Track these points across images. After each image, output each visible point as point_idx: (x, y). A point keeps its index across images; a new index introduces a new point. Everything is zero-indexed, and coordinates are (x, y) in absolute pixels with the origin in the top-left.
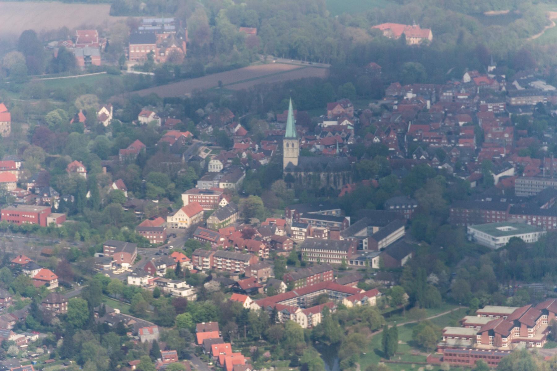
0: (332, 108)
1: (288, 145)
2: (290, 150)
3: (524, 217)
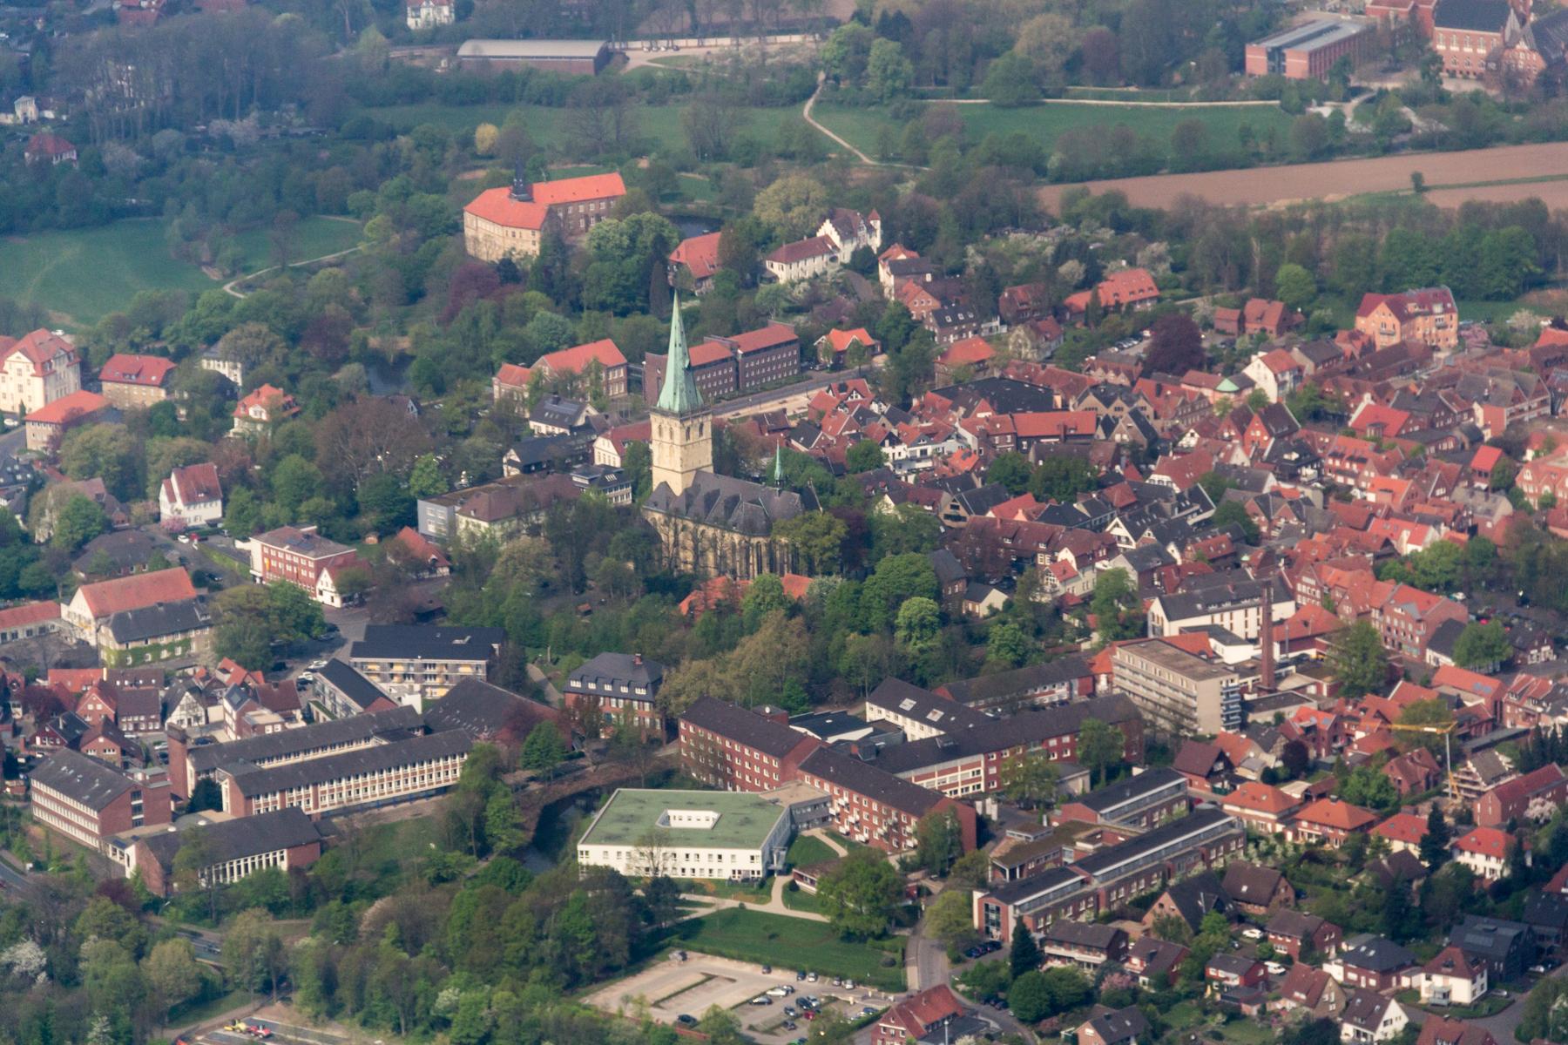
0: (1366, 314)
1: (660, 433)
2: (667, 451)
3: (827, 787)
